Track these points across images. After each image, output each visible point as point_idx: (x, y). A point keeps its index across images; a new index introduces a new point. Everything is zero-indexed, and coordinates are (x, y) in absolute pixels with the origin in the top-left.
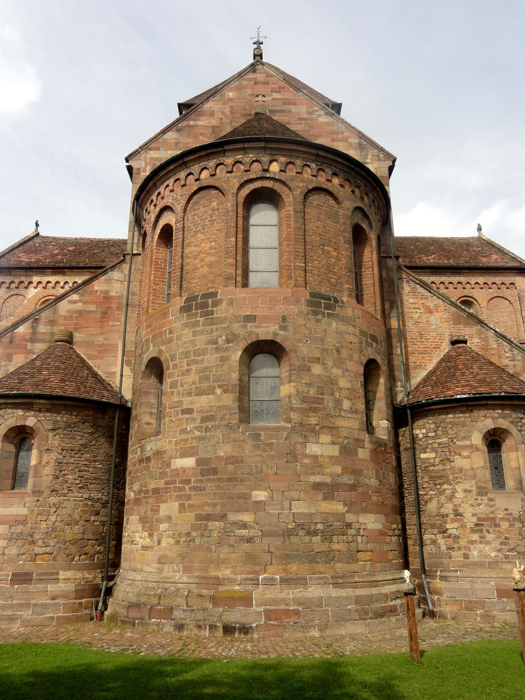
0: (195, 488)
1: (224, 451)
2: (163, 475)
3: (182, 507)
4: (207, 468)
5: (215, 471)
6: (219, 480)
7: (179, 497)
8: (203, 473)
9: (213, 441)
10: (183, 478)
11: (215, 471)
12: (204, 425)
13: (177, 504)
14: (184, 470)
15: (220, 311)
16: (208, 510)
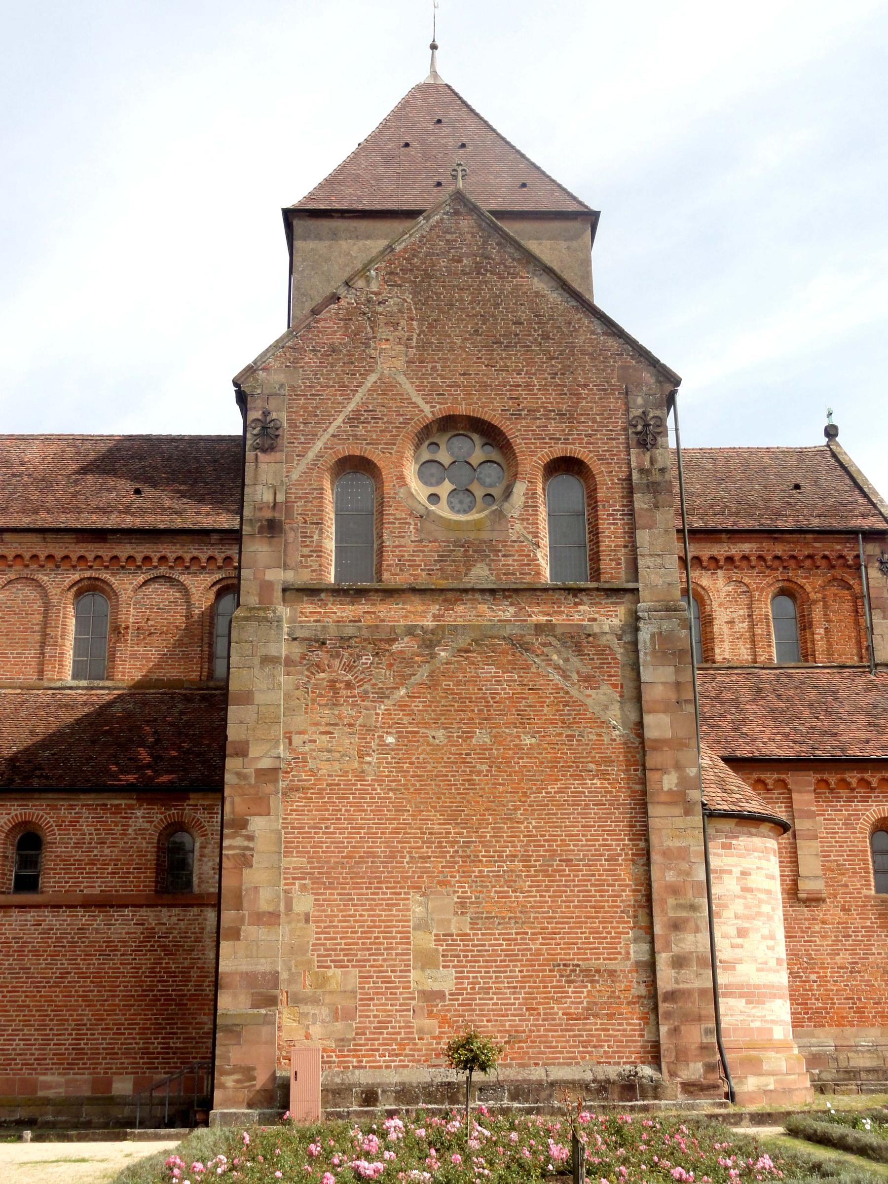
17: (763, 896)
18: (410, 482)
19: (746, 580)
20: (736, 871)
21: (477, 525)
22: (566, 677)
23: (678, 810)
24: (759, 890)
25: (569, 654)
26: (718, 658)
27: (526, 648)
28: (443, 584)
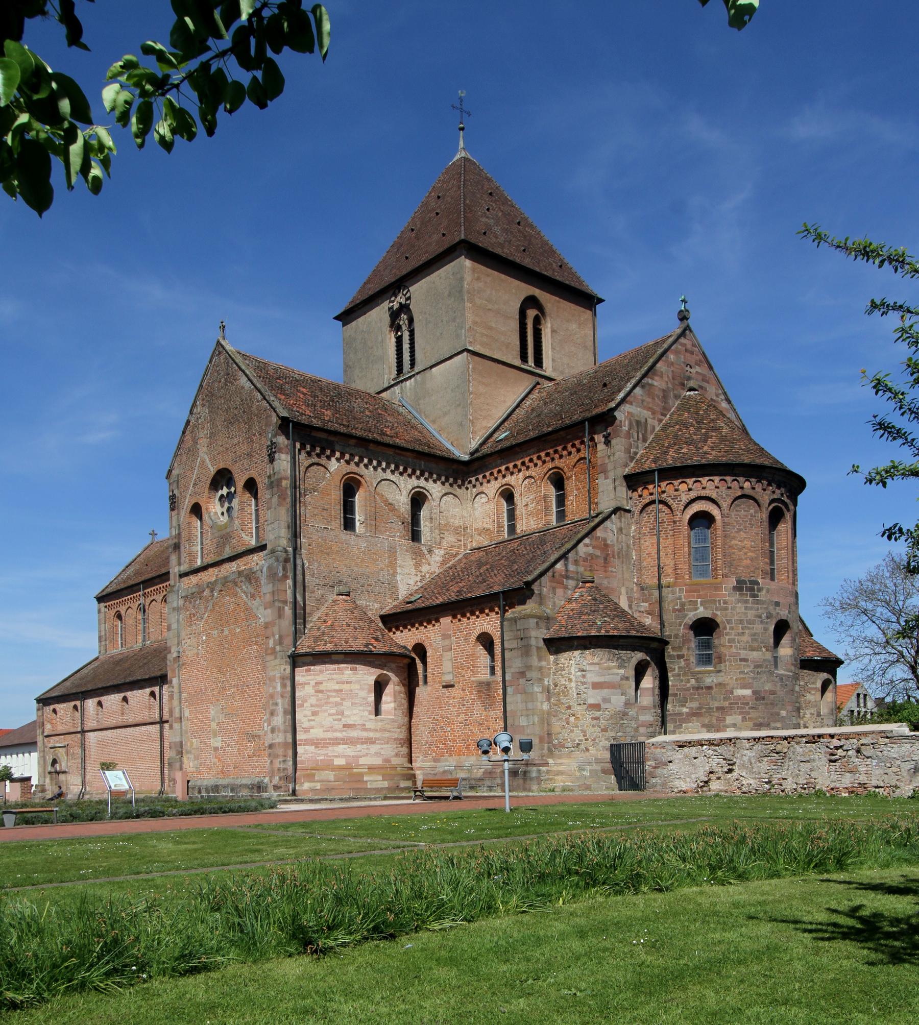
0: (752, 708)
1: (768, 687)
2: (725, 699)
3: (744, 719)
4: (758, 696)
5: (763, 698)
6: (766, 704)
7: (741, 713)
8: (757, 699)
9: (762, 680)
10: (744, 701)
11: (763, 698)
12: (756, 670)
13: (740, 717)
14: (744, 697)
15: (762, 596)
16: (761, 721)
17: (334, 694)
18: (214, 509)
19: (533, 474)
20: (312, 683)
21: (226, 526)
22: (247, 596)
23: (273, 657)
24: (329, 691)
25: (247, 584)
26: (519, 531)
27: (236, 584)
28: (218, 559)
